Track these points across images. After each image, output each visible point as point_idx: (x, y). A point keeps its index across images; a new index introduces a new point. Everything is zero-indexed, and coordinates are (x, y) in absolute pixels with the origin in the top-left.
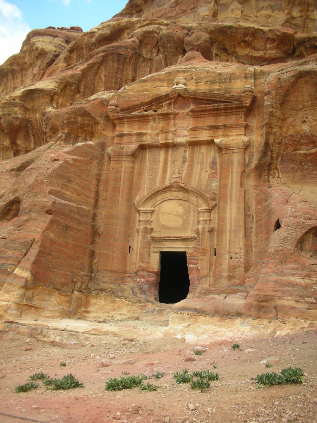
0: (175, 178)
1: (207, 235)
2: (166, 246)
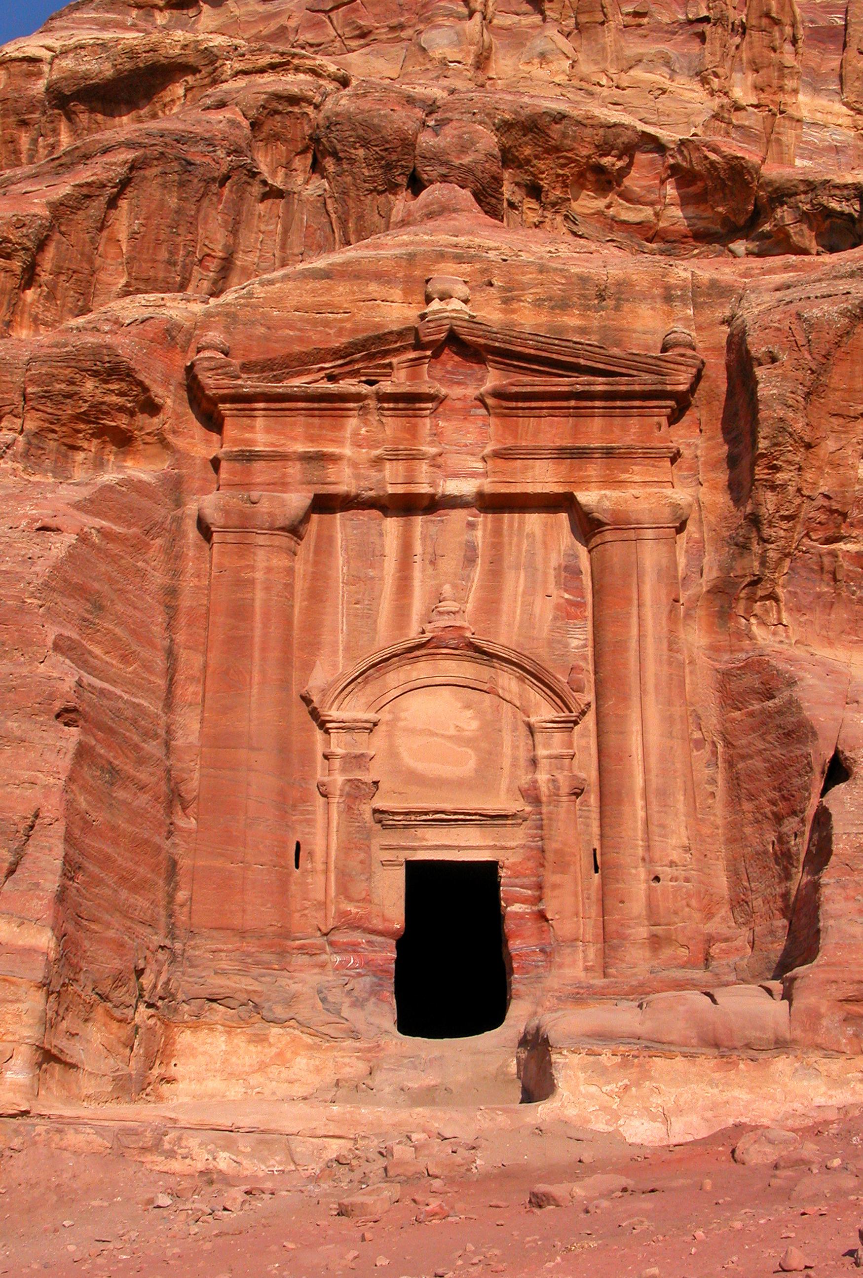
0: (448, 613)
1: (564, 805)
2: (425, 843)
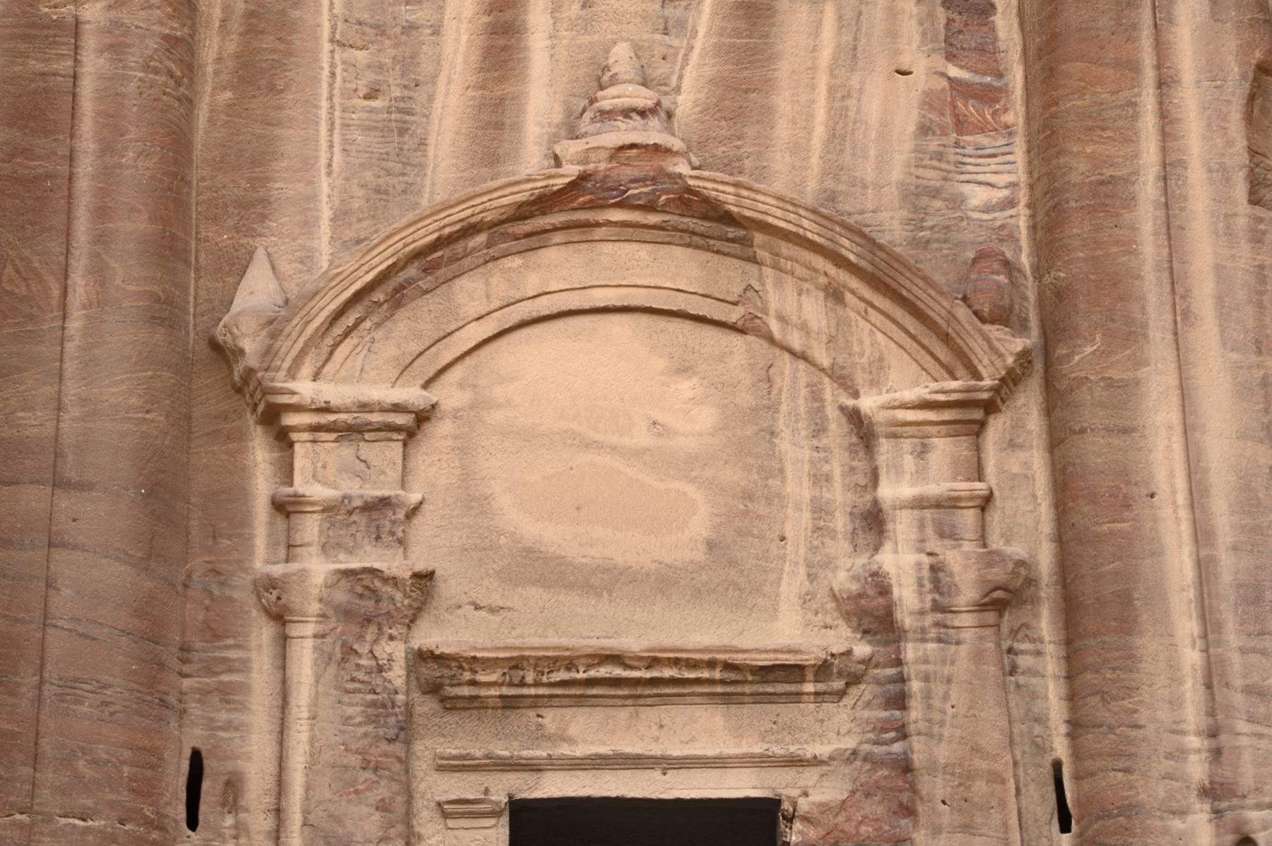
0: (627, 113)
1: (967, 635)
2: (565, 750)
